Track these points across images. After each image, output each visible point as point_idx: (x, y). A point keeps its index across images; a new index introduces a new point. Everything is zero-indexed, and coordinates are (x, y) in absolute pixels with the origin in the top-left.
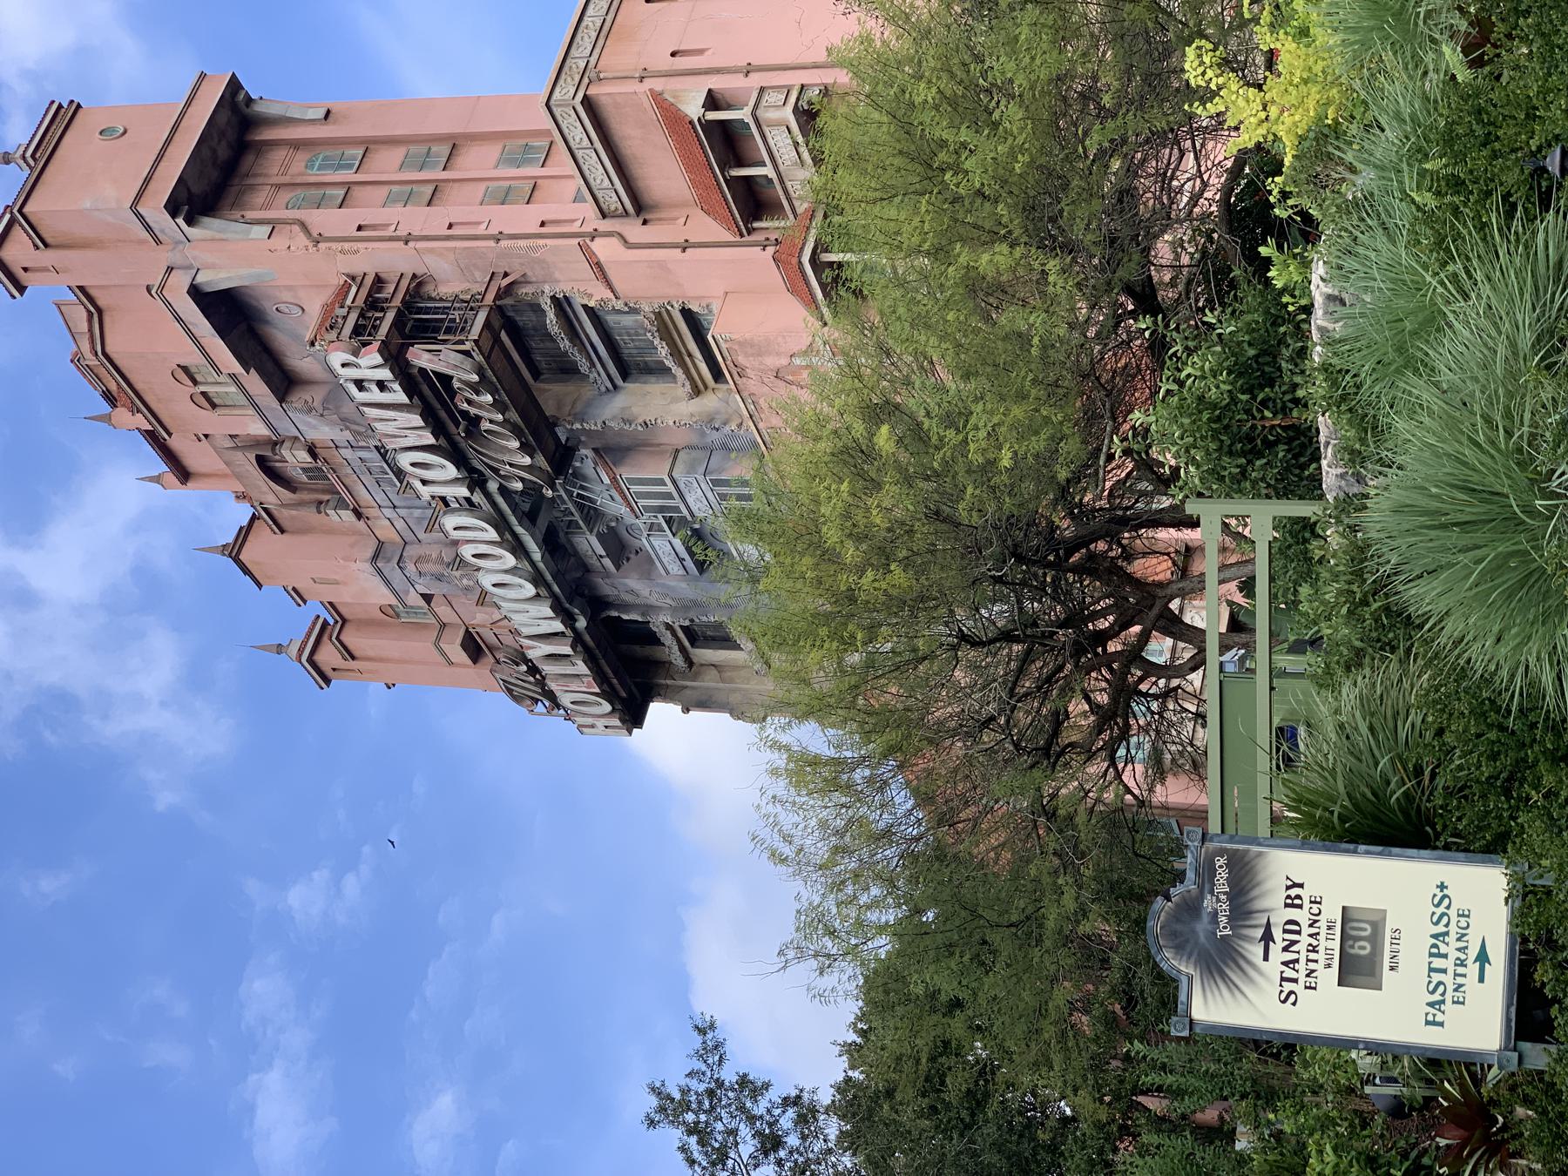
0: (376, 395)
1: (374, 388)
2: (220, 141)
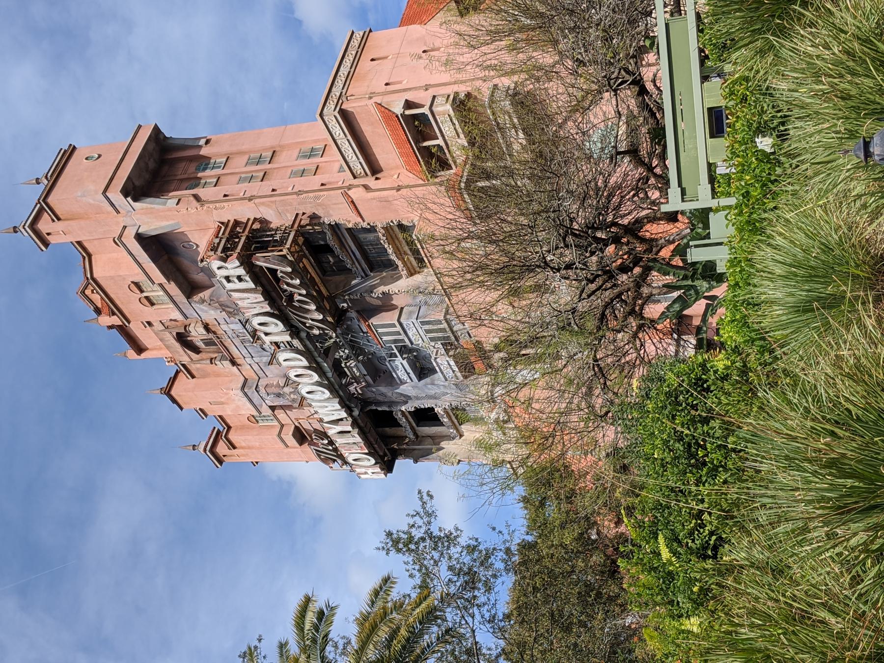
1: (236, 281)
2: (149, 159)
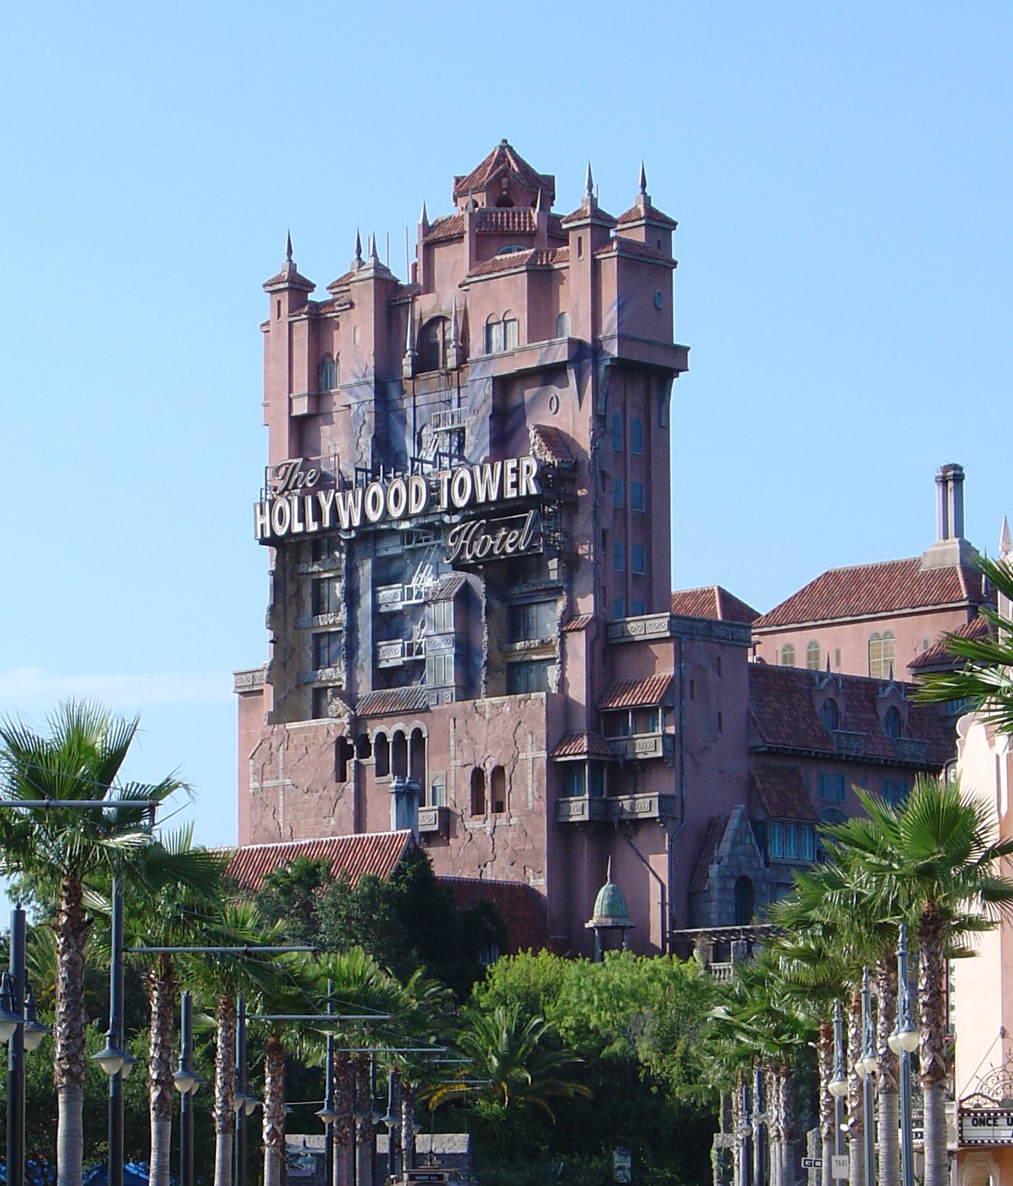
1: (514, 480)
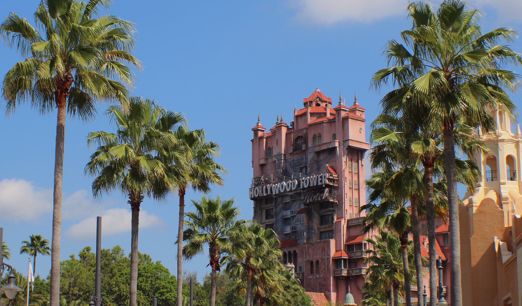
0: (319, 180)
1: (321, 180)
